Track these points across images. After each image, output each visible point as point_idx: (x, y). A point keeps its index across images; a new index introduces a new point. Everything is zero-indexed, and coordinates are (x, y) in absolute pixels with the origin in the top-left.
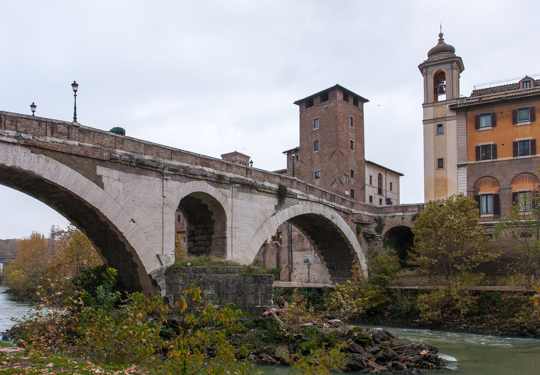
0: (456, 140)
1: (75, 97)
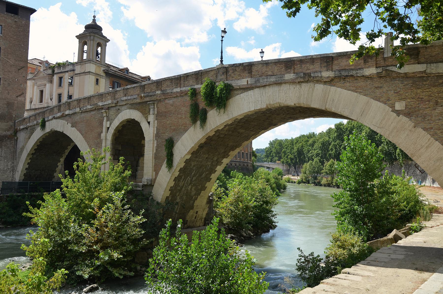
1: (222, 42)
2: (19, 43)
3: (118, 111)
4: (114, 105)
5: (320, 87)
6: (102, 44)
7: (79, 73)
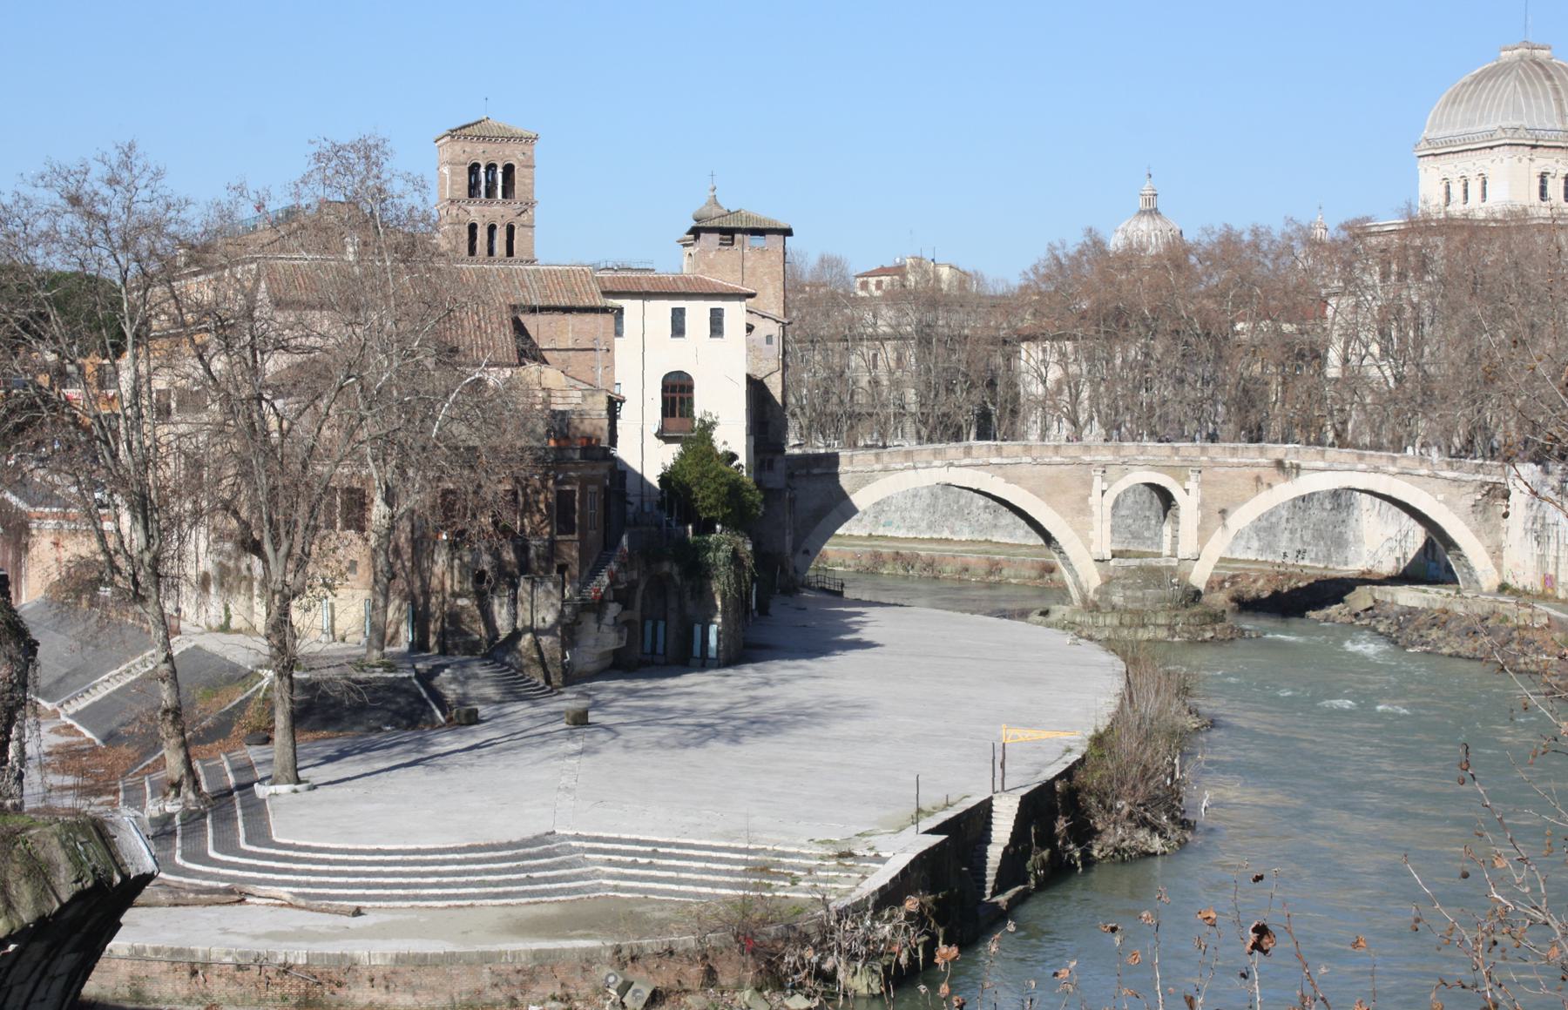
3: (1125, 472)
5: (1385, 477)
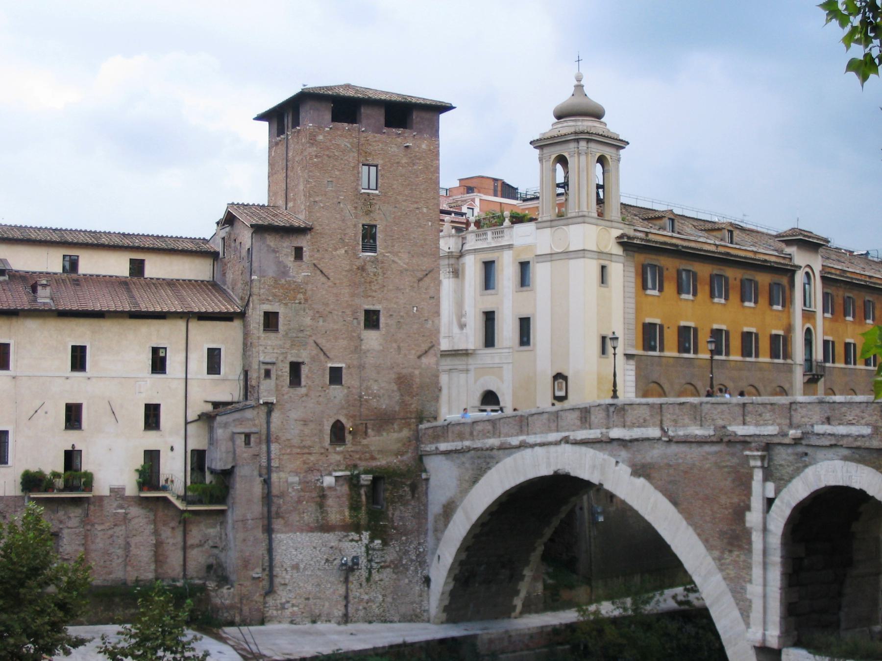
0: (622, 304)
2: (416, 206)
3: (803, 461)
4: (786, 441)
6: (608, 157)
7: (549, 252)
